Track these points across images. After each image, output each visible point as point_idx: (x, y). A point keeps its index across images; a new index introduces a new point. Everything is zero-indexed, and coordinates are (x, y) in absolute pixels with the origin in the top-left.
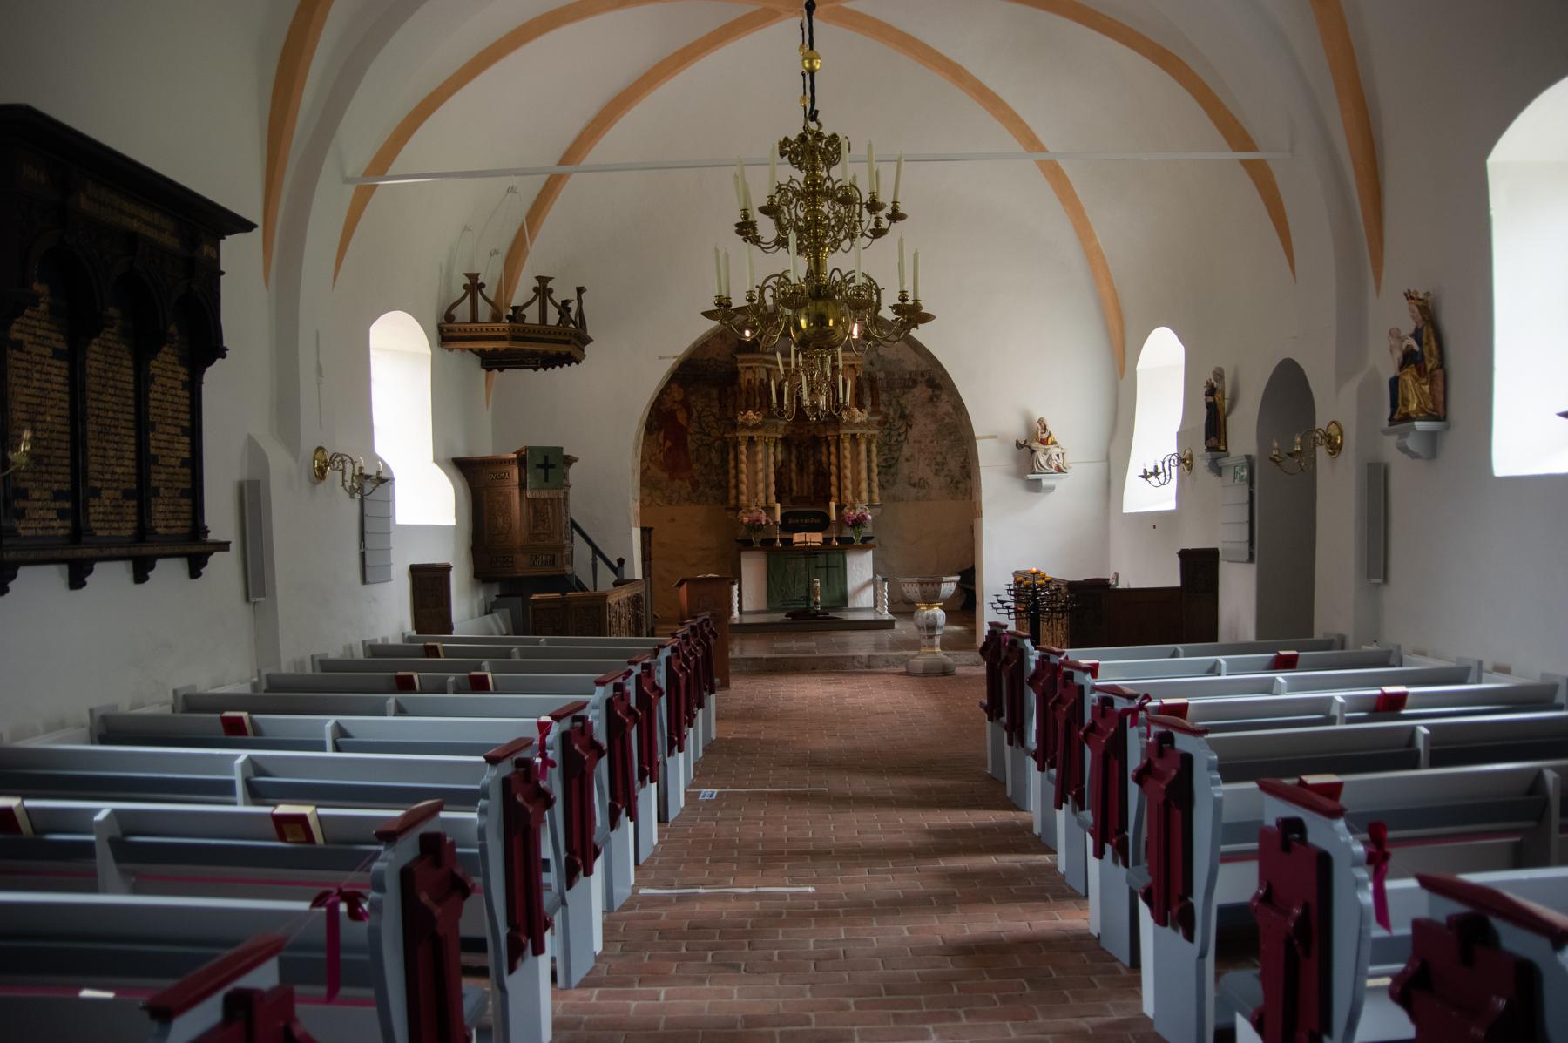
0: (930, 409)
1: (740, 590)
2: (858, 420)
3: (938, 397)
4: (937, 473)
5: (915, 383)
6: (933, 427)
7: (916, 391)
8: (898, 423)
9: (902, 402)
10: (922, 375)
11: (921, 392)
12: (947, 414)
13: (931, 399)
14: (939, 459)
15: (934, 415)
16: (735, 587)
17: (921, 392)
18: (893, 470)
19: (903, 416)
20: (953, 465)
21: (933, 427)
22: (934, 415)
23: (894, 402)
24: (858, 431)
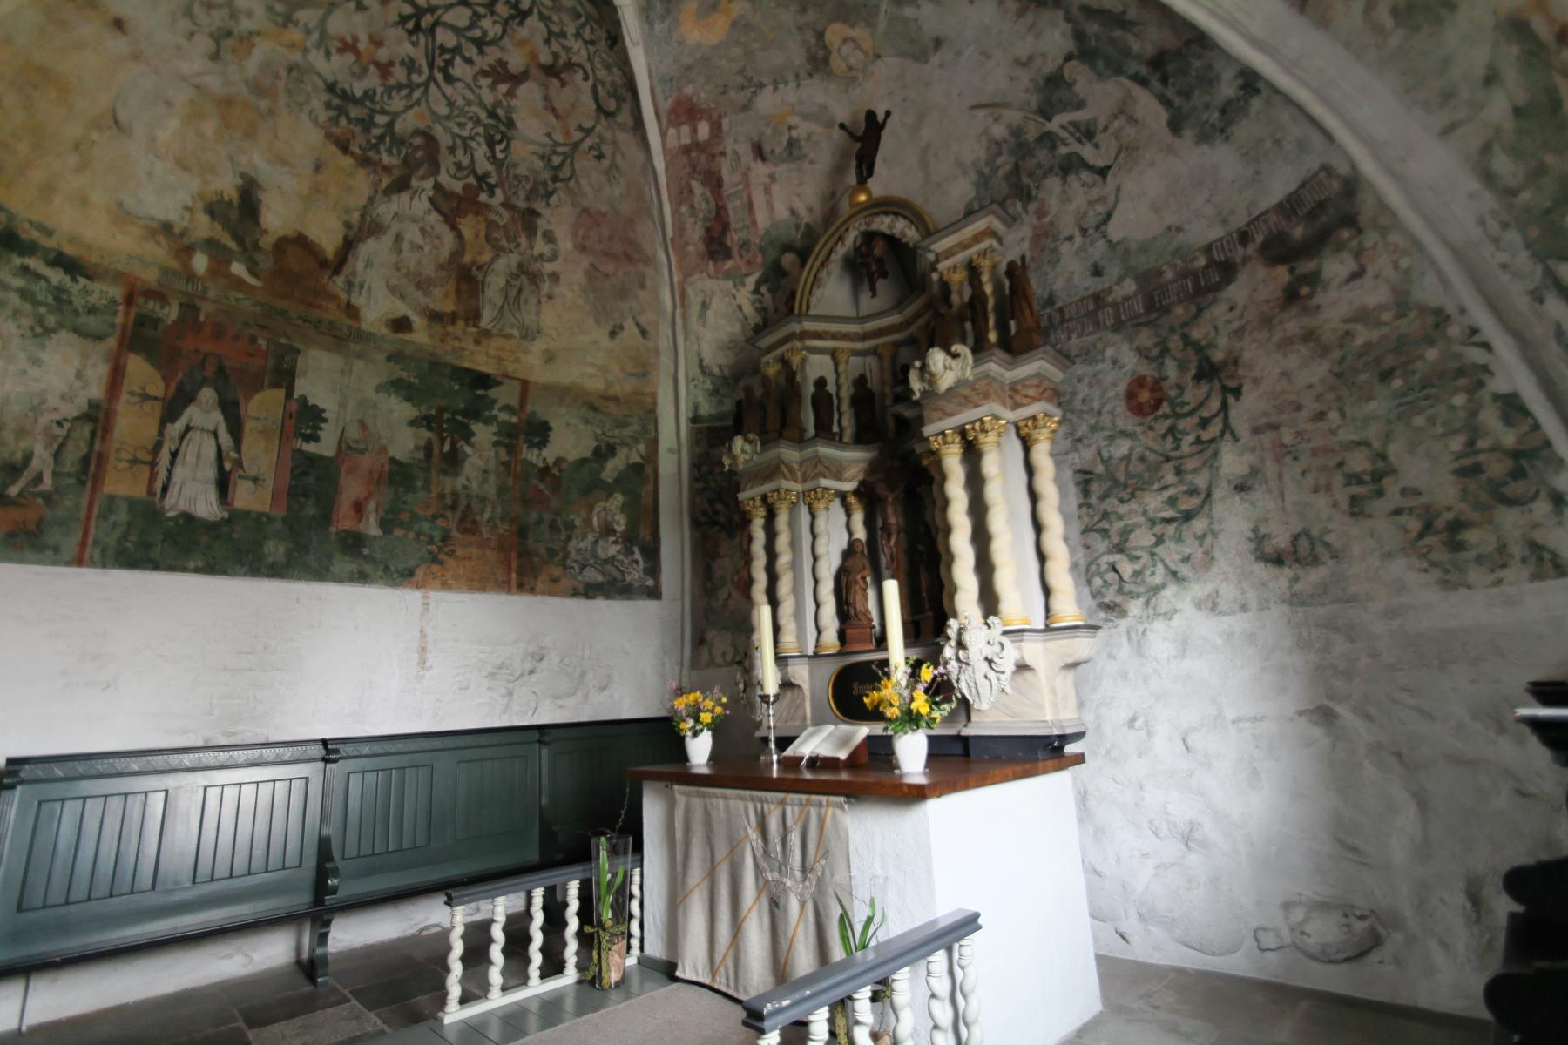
0: (1292, 324)
1: (642, 876)
2: (946, 381)
3: (1314, 279)
4: (1356, 508)
5: (1227, 271)
6: (1320, 370)
7: (1237, 292)
8: (1192, 395)
9: (1196, 334)
10: (1244, 237)
11: (1257, 284)
12: (1363, 316)
13: (1291, 296)
14: (1359, 462)
15: (1309, 336)
16: (637, 871)
17: (1257, 284)
18: (1199, 525)
19: (1208, 372)
20: (1426, 471)
21: (1320, 370)
22: (1309, 336)
23: (1175, 343)
24: (965, 417)
